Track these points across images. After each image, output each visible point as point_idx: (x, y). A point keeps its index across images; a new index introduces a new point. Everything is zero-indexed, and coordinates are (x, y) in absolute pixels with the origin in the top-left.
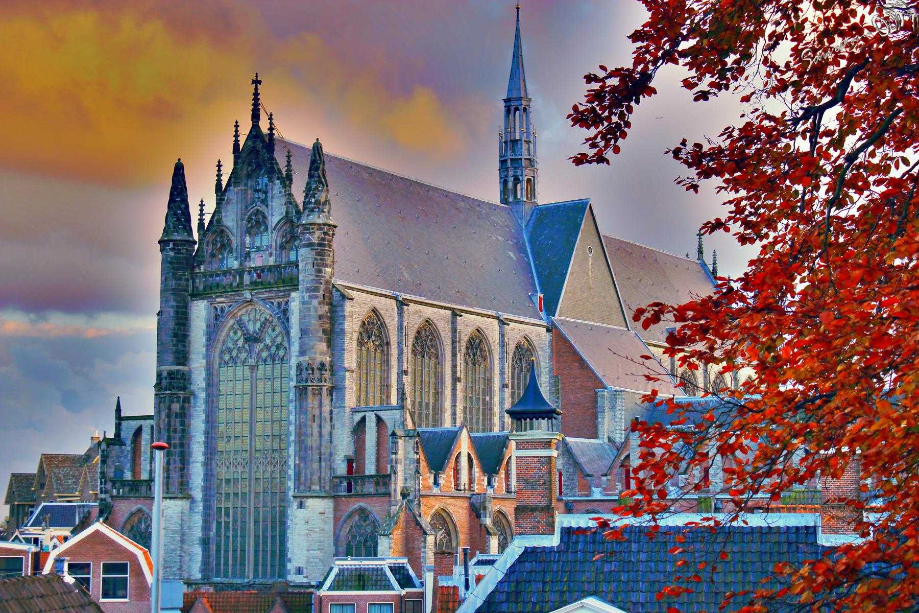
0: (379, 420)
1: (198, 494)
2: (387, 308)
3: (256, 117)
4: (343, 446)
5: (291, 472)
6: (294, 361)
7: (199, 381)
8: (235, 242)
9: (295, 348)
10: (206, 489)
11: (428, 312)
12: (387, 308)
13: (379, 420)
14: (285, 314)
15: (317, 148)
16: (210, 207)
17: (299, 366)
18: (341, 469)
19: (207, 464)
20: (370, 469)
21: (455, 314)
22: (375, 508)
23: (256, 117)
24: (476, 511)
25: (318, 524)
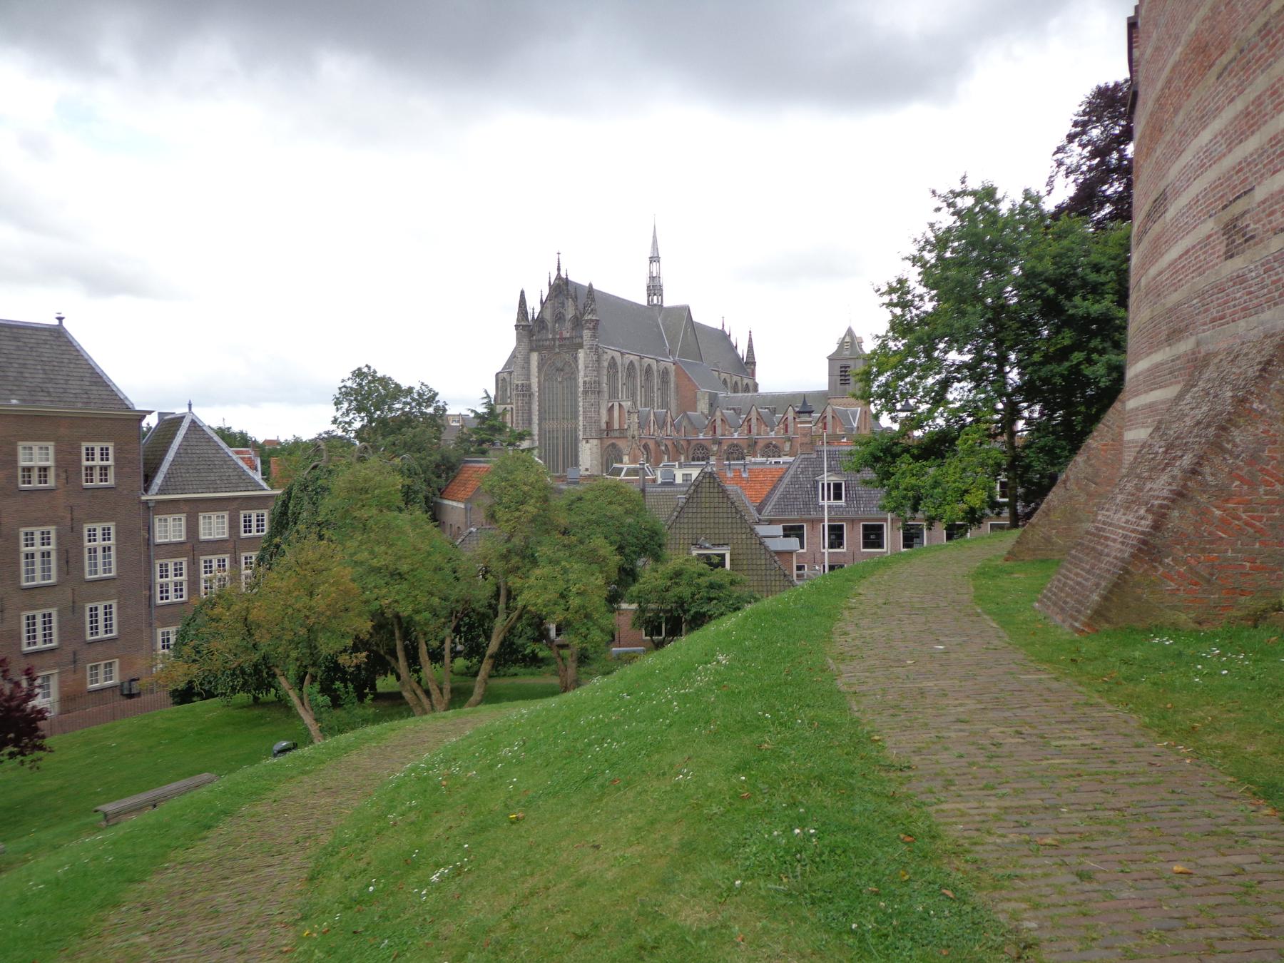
0: (620, 405)
1: (536, 438)
2: (617, 355)
3: (559, 269)
4: (604, 418)
5: (581, 428)
6: (581, 381)
7: (535, 388)
8: (550, 325)
9: (582, 374)
10: (539, 435)
11: (632, 357)
12: (617, 355)
13: (620, 405)
14: (576, 359)
15: (591, 285)
16: (538, 309)
17: (585, 382)
18: (604, 426)
19: (539, 424)
20: (616, 426)
21: (641, 358)
22: (621, 444)
23: (559, 269)
24: (658, 444)
25: (595, 450)
